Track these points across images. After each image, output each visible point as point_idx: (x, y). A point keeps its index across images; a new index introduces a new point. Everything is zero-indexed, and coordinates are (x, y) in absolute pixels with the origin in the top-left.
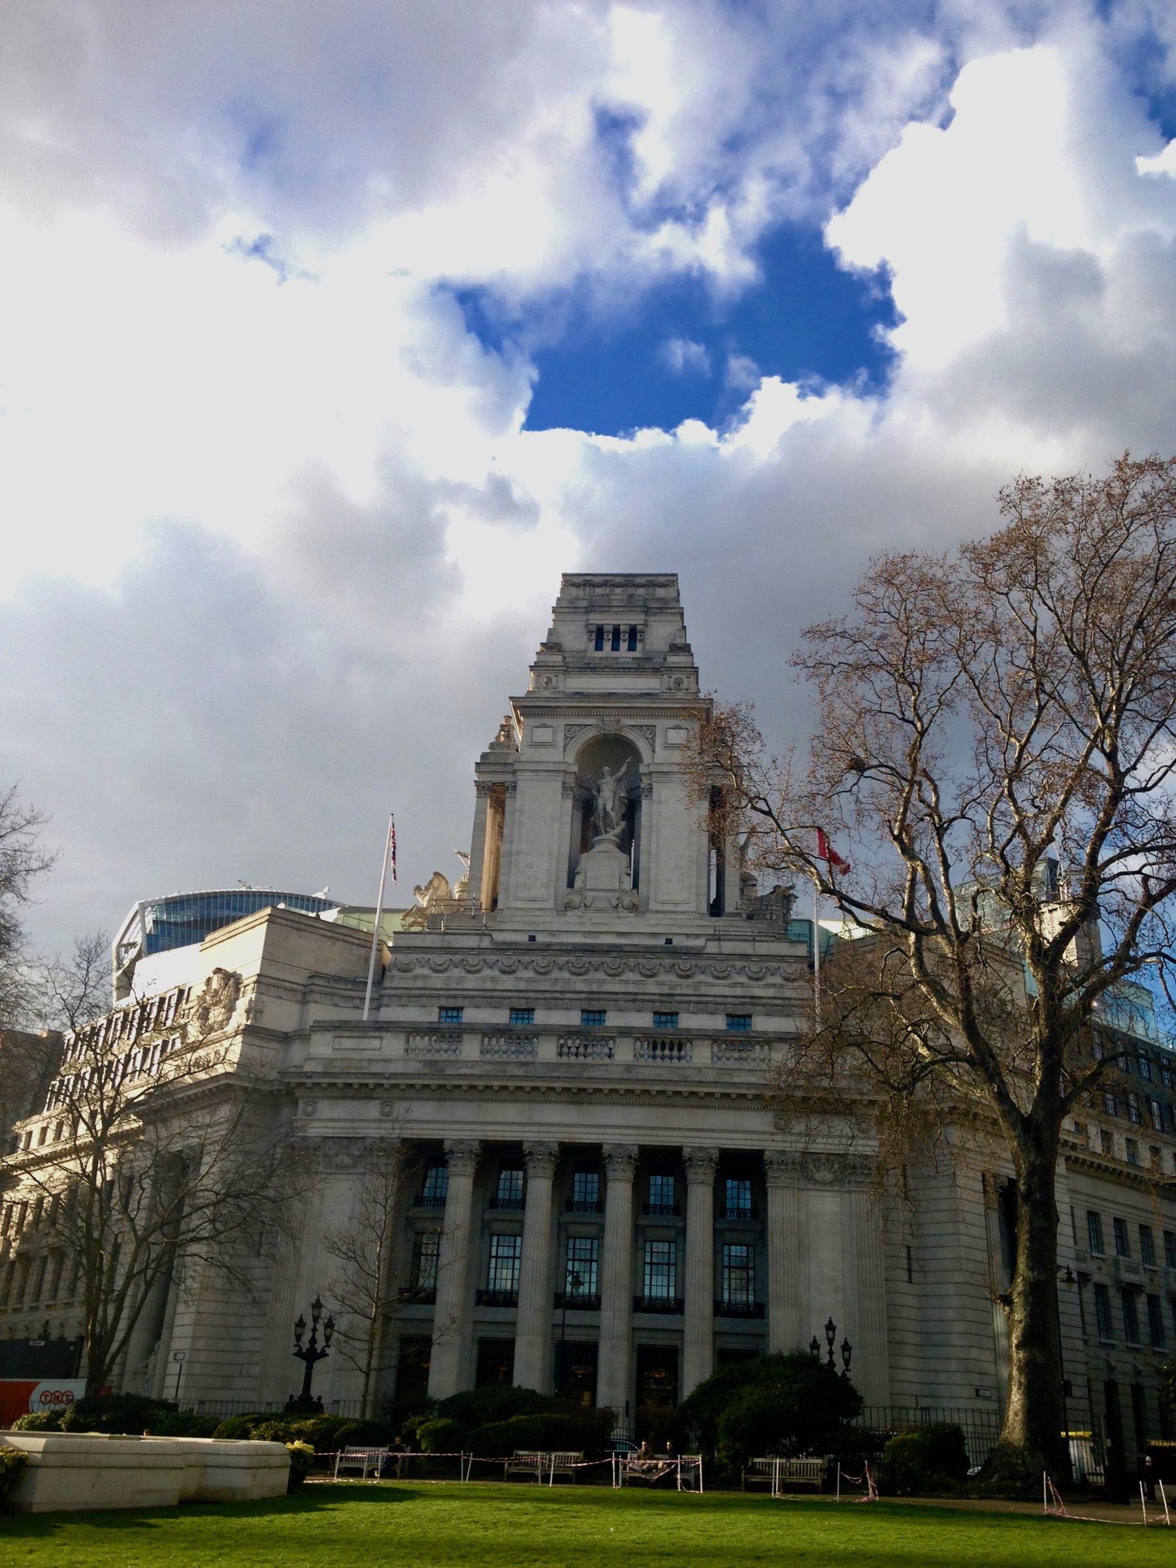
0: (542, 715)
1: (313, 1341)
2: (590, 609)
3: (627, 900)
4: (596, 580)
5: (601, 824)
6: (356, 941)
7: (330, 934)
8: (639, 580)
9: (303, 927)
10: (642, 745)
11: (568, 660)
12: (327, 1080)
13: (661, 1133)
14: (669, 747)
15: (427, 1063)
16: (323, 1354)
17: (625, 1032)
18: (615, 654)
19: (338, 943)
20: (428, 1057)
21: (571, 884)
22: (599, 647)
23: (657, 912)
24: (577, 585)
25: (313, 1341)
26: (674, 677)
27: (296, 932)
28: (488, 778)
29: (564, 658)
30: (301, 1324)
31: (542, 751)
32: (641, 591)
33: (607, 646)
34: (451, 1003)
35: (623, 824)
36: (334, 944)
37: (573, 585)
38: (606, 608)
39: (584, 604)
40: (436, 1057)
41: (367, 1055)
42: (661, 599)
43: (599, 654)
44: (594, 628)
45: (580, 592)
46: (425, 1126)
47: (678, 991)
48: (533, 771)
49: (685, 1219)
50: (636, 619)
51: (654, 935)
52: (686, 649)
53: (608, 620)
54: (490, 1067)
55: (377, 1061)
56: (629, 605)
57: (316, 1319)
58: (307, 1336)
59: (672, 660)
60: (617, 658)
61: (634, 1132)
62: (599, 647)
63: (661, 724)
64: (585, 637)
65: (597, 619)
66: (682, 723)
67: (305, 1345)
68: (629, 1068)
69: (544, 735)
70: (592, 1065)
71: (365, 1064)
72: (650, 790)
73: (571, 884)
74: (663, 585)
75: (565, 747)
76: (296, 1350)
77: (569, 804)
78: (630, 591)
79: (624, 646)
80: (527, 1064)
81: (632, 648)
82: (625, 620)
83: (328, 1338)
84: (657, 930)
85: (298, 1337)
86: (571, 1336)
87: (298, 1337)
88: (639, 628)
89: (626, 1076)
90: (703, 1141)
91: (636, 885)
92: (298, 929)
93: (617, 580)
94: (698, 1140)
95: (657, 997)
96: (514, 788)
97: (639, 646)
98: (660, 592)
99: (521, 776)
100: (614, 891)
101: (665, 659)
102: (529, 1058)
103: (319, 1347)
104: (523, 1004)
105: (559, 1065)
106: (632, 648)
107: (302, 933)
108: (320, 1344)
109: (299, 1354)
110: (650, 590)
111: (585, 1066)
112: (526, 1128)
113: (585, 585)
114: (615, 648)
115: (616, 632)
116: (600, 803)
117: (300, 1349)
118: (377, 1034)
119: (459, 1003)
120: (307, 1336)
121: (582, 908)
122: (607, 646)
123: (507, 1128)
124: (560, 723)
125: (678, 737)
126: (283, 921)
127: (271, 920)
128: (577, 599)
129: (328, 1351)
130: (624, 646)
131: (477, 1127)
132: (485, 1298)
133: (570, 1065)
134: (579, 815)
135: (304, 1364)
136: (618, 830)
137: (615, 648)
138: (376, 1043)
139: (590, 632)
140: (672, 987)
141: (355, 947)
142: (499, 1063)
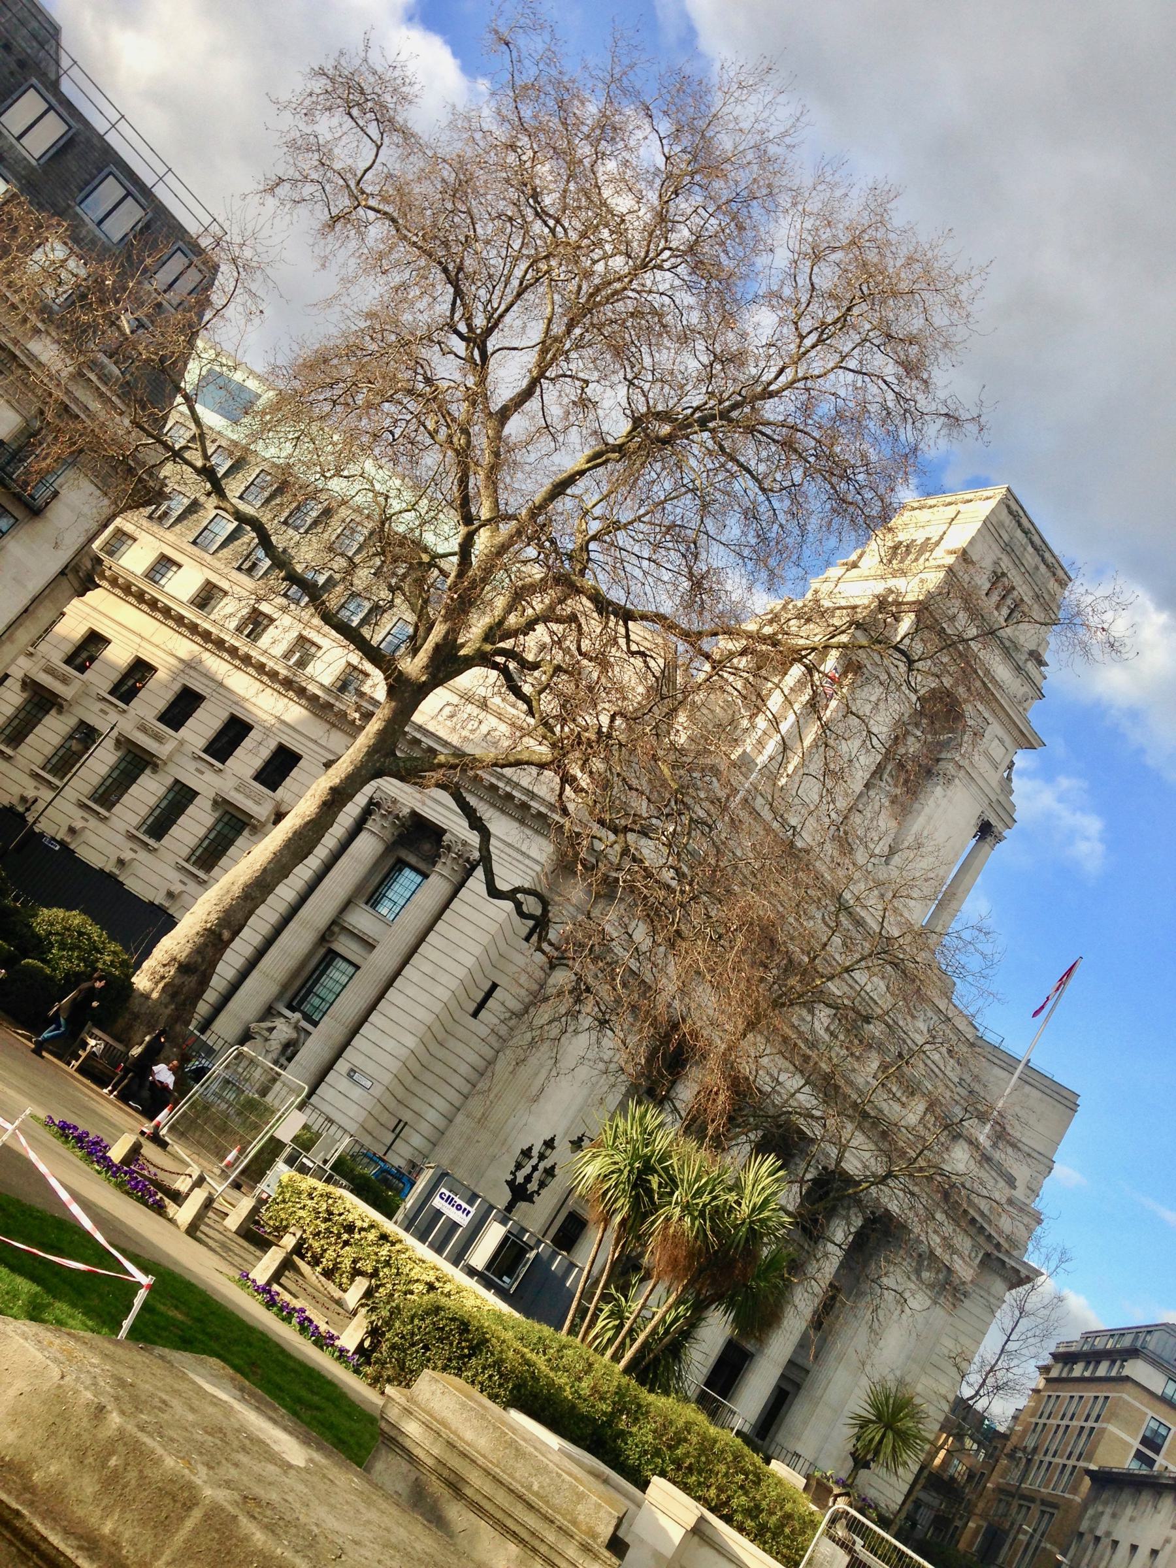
1: (528, 1178)
2: (1008, 548)
4: (1024, 521)
8: (1047, 555)
16: (529, 1199)
24: (1011, 512)
30: (527, 1153)
32: (1043, 568)
37: (1008, 507)
38: (1018, 562)
52: (1041, 663)
56: (1029, 574)
57: (542, 1157)
59: (1031, 666)
65: (1006, 563)
66: (1008, 741)
76: (510, 1177)
78: (1038, 559)
82: (1023, 590)
85: (519, 1166)
87: (519, 1166)
93: (1036, 539)
98: (1052, 585)
108: (532, 1187)
109: (511, 1183)
114: (997, 608)
120: (527, 1170)
137: (997, 608)
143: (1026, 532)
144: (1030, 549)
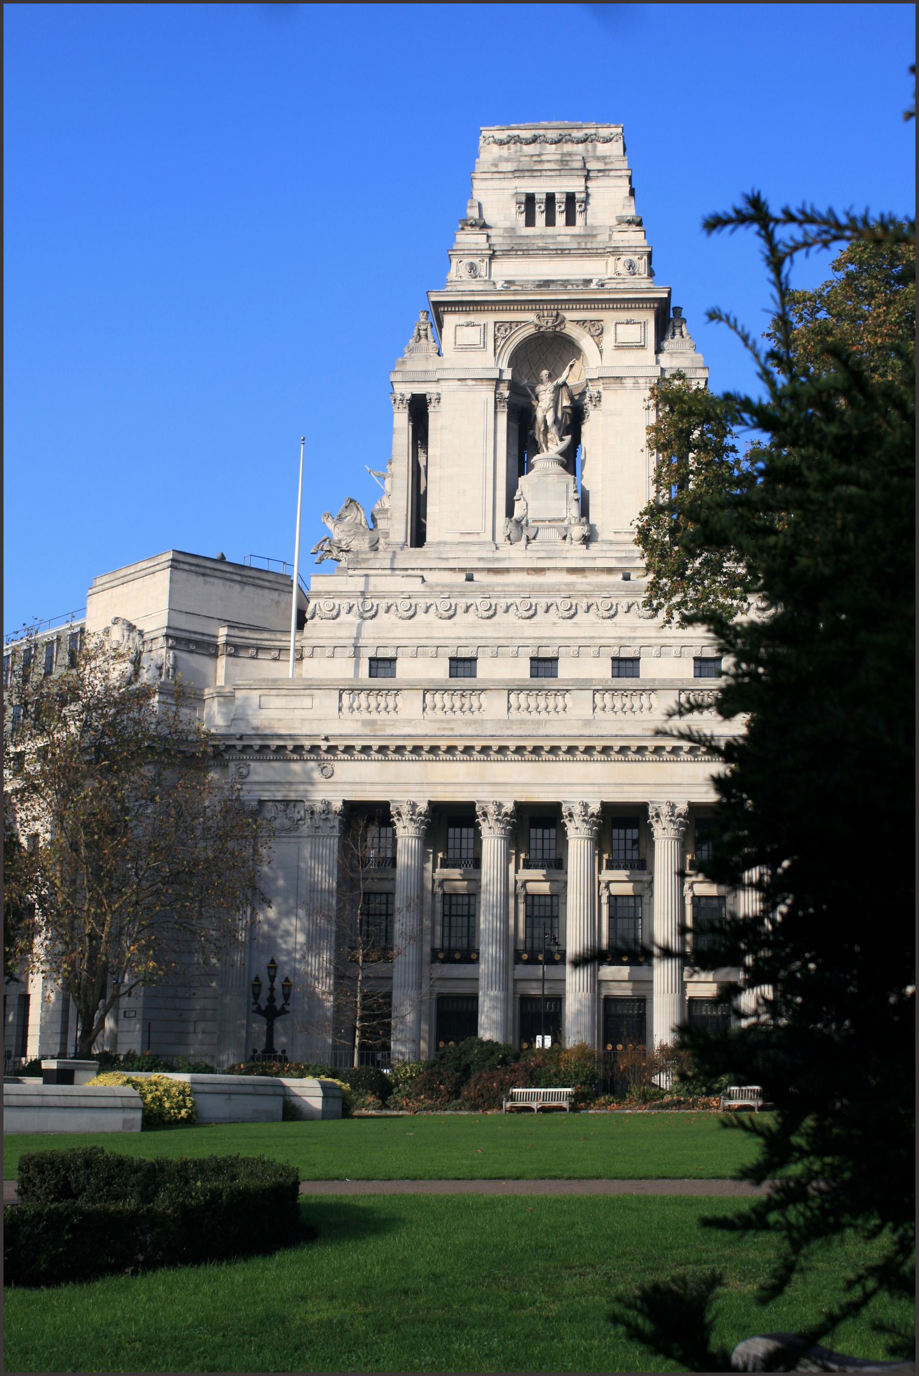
0: (467, 312)
1: (271, 999)
2: (519, 173)
3: (578, 531)
5: (540, 438)
6: (267, 584)
7: (238, 578)
9: (208, 572)
10: (586, 343)
11: (493, 240)
12: (259, 742)
13: (626, 788)
14: (618, 347)
15: (365, 723)
16: (283, 1011)
17: (582, 685)
18: (550, 229)
19: (247, 588)
20: (366, 716)
21: (510, 512)
22: (530, 222)
23: (611, 543)
24: (501, 143)
25: (271, 999)
26: (624, 258)
27: (201, 579)
28: (406, 390)
29: (488, 237)
31: (471, 355)
32: (581, 147)
33: (540, 219)
34: (382, 654)
35: (568, 438)
36: (243, 589)
39: (509, 167)
40: (374, 716)
41: (299, 714)
42: (604, 158)
43: (530, 231)
44: (523, 199)
45: (504, 151)
46: (368, 788)
47: (638, 634)
48: (459, 380)
49: (651, 873)
50: (575, 185)
51: (610, 570)
53: (540, 187)
54: (437, 725)
55: (311, 721)
56: (564, 166)
58: (264, 994)
60: (554, 237)
61: (596, 789)
62: (530, 222)
63: (608, 317)
64: (514, 208)
67: (264, 1004)
68: (587, 723)
69: (472, 336)
70: (547, 721)
71: (297, 724)
72: (599, 398)
73: (510, 512)
74: (607, 141)
75: (495, 350)
76: (254, 1007)
77: (503, 419)
78: (568, 148)
79: (560, 219)
80: (475, 722)
81: (570, 222)
82: (561, 186)
83: (286, 996)
84: (613, 564)
86: (534, 990)
87: (256, 996)
88: (578, 196)
89: (586, 732)
90: (671, 795)
91: (584, 511)
92: (204, 575)
94: (667, 795)
95: (613, 641)
96: (439, 400)
97: (579, 219)
98: (602, 149)
99: (442, 388)
100: (563, 520)
101: (610, 236)
102: (477, 715)
103: (279, 1004)
104: (464, 653)
105: (509, 722)
106: (570, 222)
107: (209, 579)
109: (259, 1011)
110: (590, 146)
111: (538, 723)
112: (479, 788)
113: (508, 142)
114: (550, 222)
115: (550, 199)
116: (539, 414)
117: (259, 1007)
118: (307, 692)
119: (390, 653)
120: (264, 994)
121: (523, 541)
122: (540, 219)
123: (457, 788)
124: (489, 319)
125: (631, 334)
126: (186, 567)
127: (175, 565)
128: (502, 159)
129: (287, 1008)
130: (560, 219)
131: (425, 788)
132: (441, 956)
133: (523, 722)
134: (515, 426)
135: (264, 1020)
136: (562, 446)
137: (550, 222)
138: (307, 702)
139: (517, 203)
140: (634, 629)
141: (266, 591)
142: (442, 721)
143: (534, 140)
144: (548, 146)
